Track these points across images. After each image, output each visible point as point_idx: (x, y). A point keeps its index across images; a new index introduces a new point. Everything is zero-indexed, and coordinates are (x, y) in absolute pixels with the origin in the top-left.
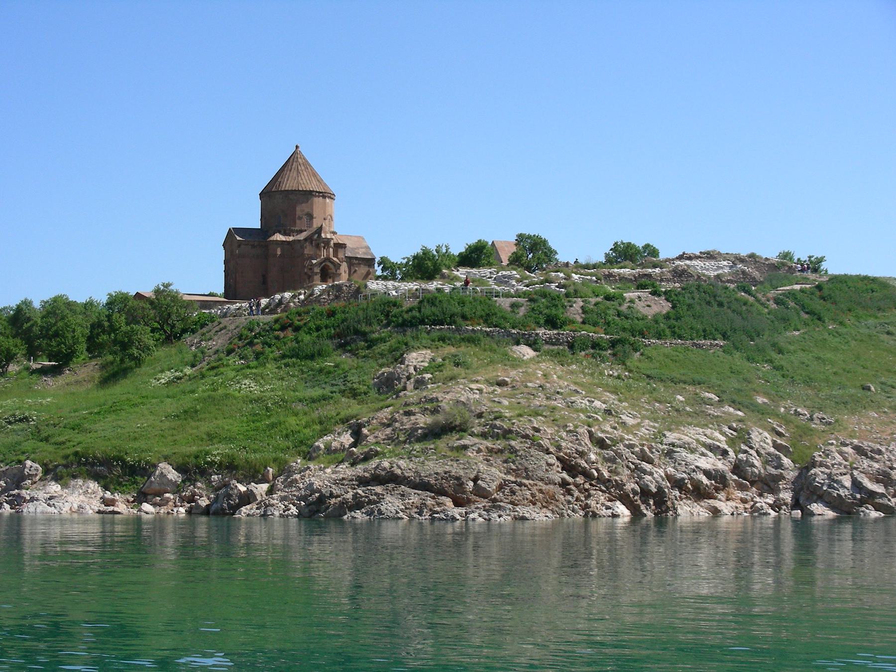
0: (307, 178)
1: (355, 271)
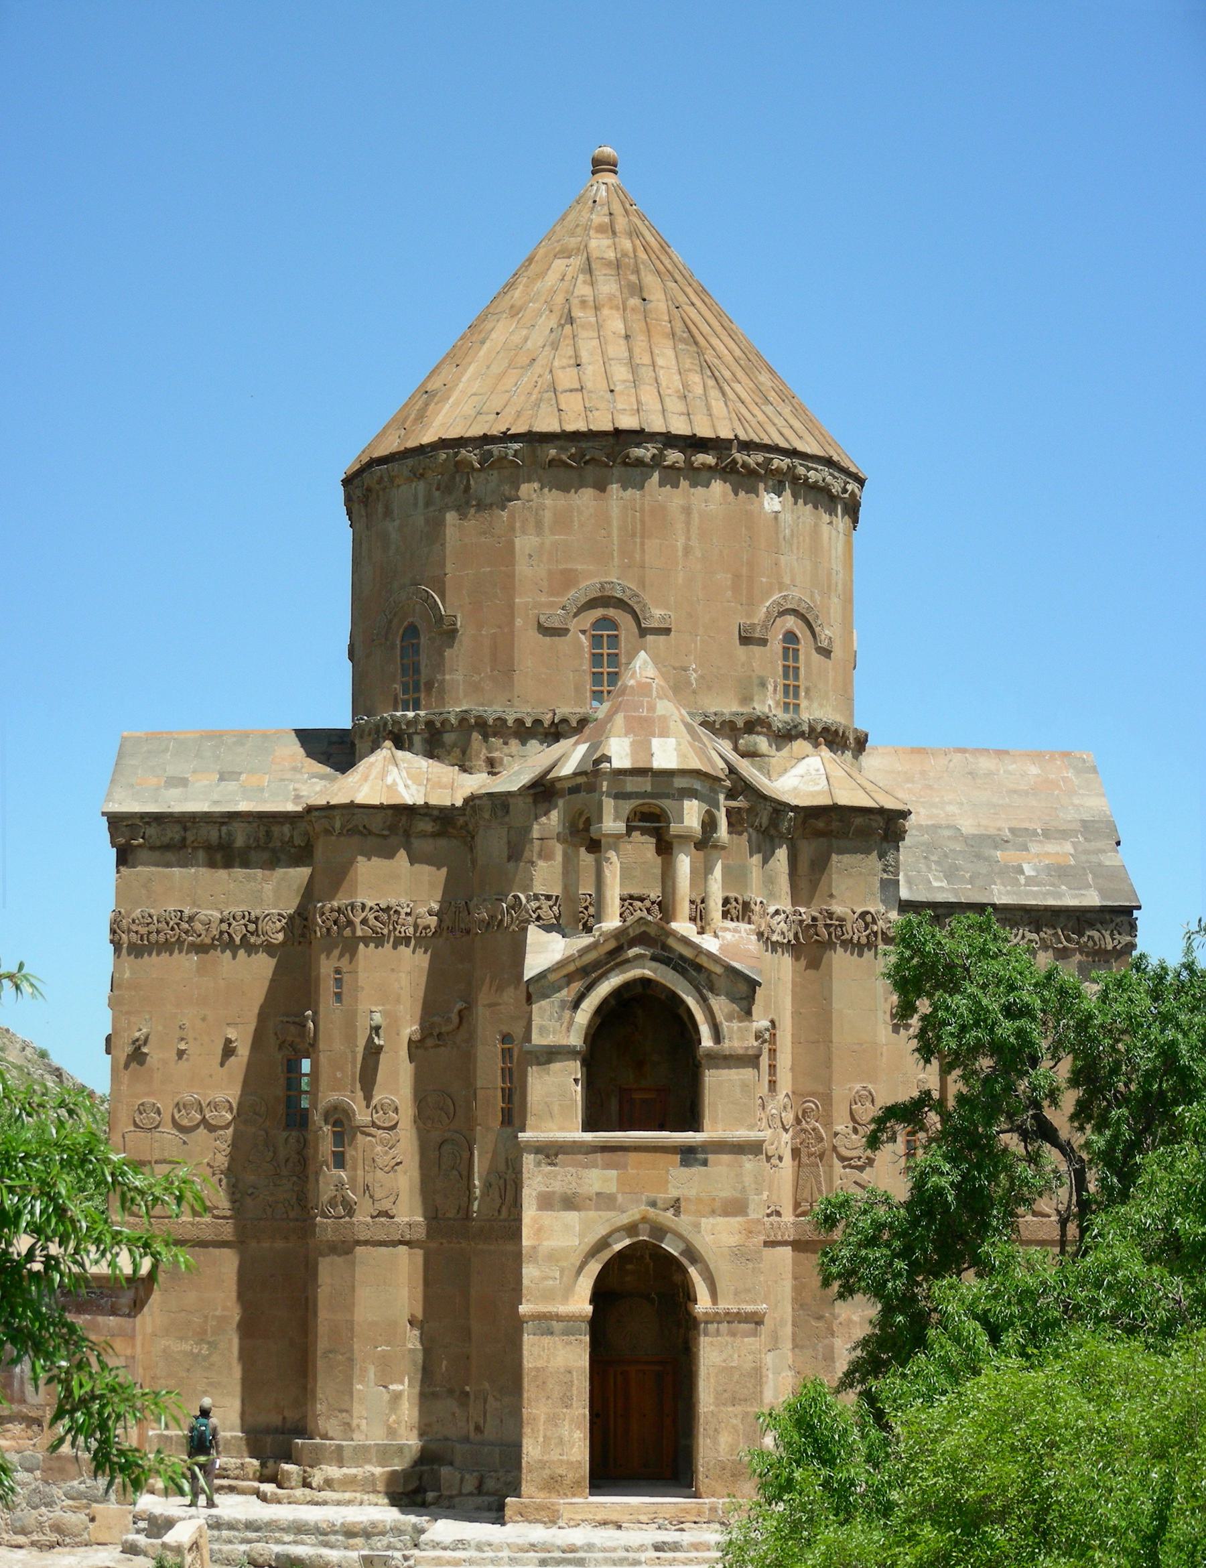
0: (618, 349)
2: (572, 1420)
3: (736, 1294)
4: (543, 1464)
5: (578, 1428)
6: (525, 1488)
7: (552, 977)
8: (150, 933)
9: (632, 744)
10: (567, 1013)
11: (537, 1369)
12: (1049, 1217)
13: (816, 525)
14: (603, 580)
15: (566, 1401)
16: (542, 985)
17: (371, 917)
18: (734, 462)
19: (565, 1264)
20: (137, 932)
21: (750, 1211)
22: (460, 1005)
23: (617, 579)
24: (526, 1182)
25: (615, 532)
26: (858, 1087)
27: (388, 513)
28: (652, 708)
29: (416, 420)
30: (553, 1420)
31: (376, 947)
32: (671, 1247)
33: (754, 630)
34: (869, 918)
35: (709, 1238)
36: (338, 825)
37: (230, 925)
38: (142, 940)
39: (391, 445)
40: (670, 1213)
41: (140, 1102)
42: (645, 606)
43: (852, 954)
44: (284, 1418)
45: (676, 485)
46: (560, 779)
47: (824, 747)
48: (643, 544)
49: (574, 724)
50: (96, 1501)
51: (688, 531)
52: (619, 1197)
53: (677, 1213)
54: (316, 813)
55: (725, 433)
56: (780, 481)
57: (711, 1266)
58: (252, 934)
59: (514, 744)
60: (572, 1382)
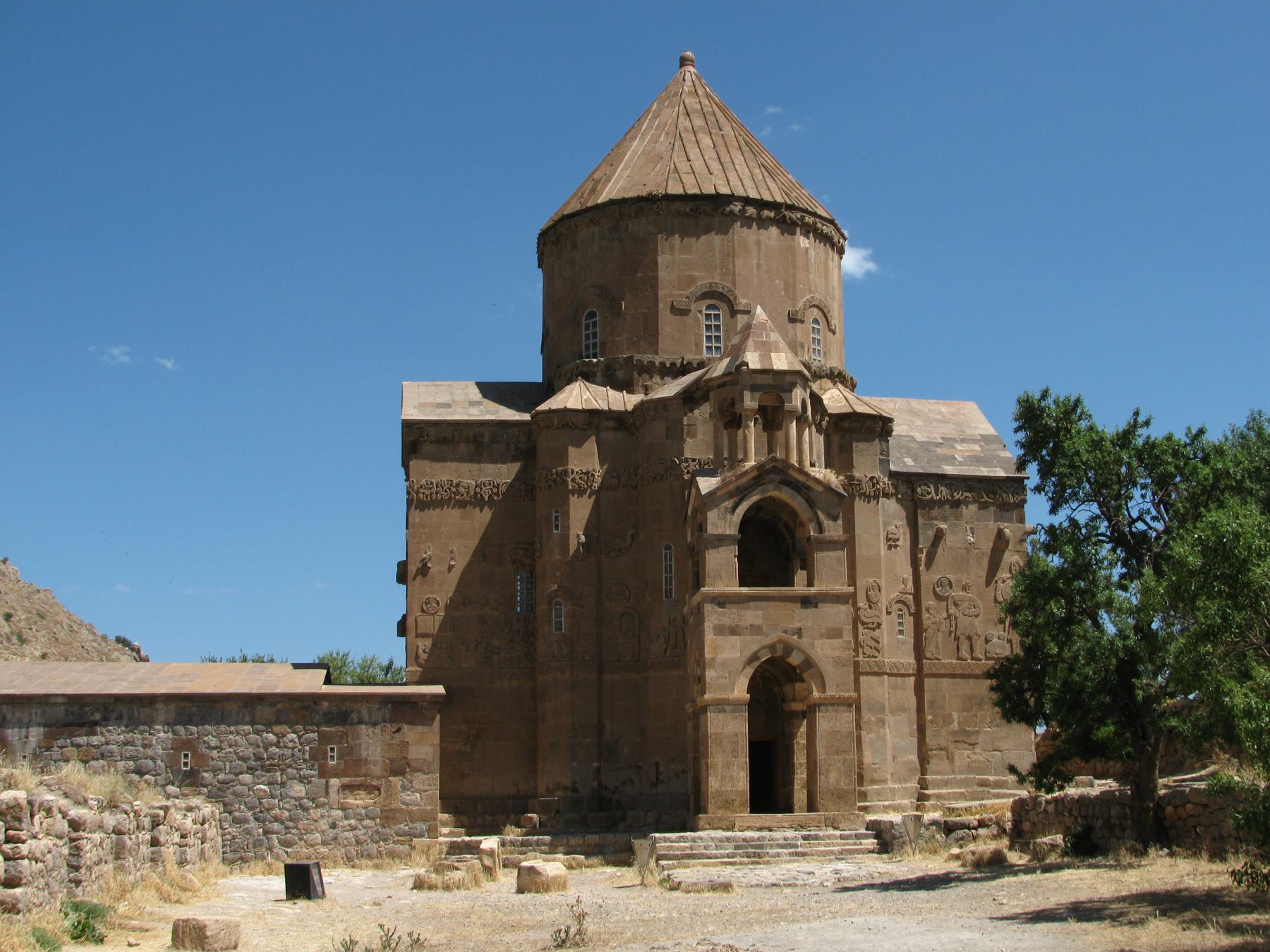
0: (710, 154)
1: (939, 536)
2: (738, 765)
3: (838, 686)
4: (719, 793)
5: (743, 770)
6: (711, 808)
7: (720, 493)
8: (431, 494)
9: (760, 355)
10: (729, 516)
11: (716, 734)
12: (981, 660)
13: (827, 259)
14: (711, 281)
15: (735, 753)
16: (712, 499)
17: (577, 477)
18: (784, 216)
19: (732, 669)
20: (423, 493)
21: (844, 635)
22: (632, 532)
23: (717, 280)
24: (707, 619)
25: (717, 255)
26: (871, 580)
27: (574, 246)
28: (768, 336)
29: (590, 194)
30: (728, 765)
31: (578, 497)
32: (795, 659)
33: (798, 314)
35: (819, 651)
36: (556, 422)
37: (481, 489)
38: (427, 497)
39: (574, 207)
40: (795, 637)
41: (427, 597)
42: (736, 297)
43: (864, 501)
44: (518, 789)
45: (750, 227)
46: (711, 380)
47: (839, 384)
48: (734, 261)
49: (695, 366)
50: (416, 837)
51: (759, 255)
52: (764, 627)
53: (800, 636)
54: (541, 416)
55: (779, 199)
56: (809, 230)
57: (822, 670)
58: (495, 494)
59: (657, 379)
60: (738, 741)
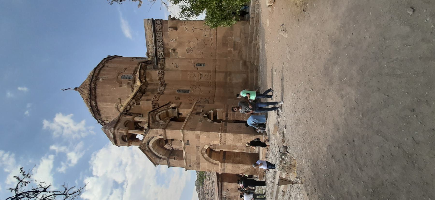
34: (159, 73)
53: (199, 146)
